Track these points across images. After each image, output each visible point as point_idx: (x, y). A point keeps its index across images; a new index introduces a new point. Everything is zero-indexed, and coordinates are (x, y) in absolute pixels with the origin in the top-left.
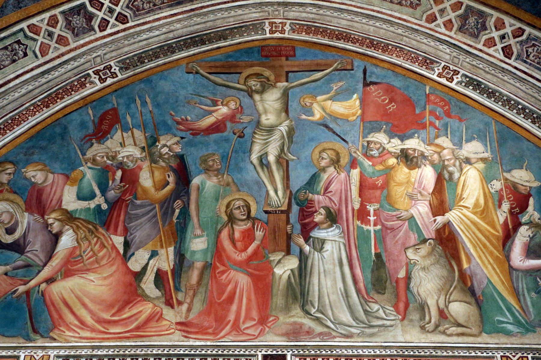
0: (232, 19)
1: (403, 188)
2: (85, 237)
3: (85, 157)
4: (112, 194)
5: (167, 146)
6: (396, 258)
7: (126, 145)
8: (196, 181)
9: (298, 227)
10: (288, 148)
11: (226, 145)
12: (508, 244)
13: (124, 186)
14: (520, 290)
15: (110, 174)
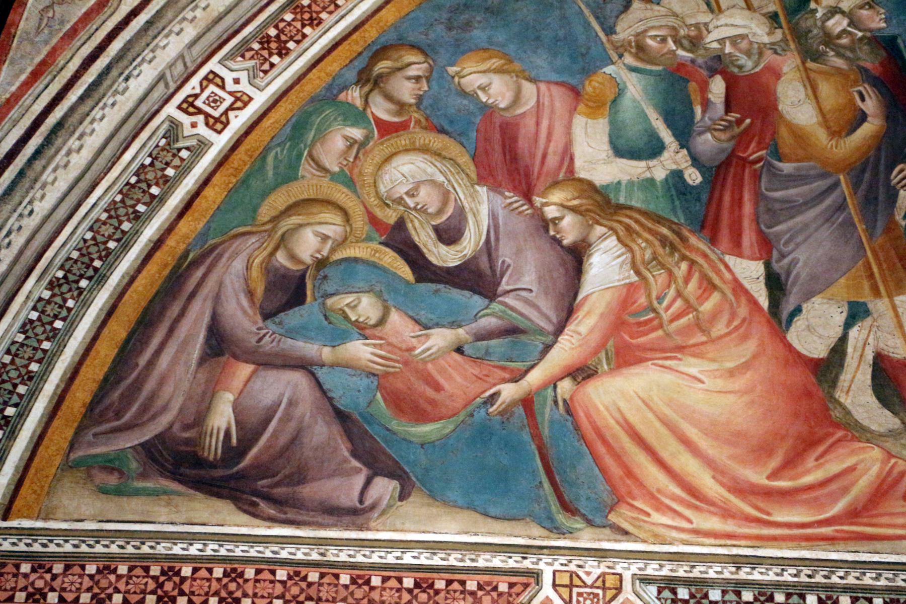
2: (655, 258)
3: (614, 37)
5: (843, 13)
7: (723, 7)
13: (739, 122)
15: (693, 86)
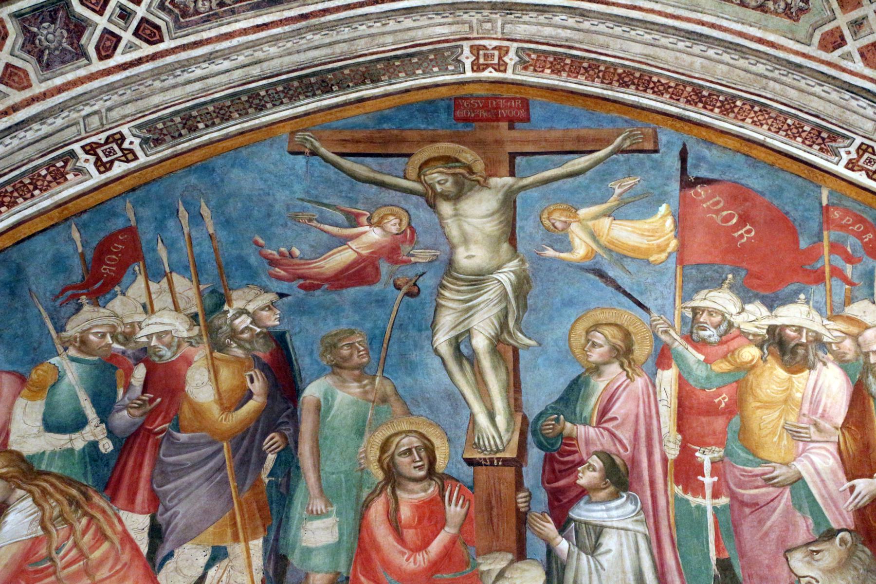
0: (389, 39)
1: (777, 414)
2: (61, 515)
3: (64, 334)
4: (123, 418)
5: (248, 313)
6: (766, 571)
7: (156, 308)
8: (312, 391)
9: (542, 497)
10: (518, 321)
11: (379, 312)
13: (151, 401)
15: (120, 372)
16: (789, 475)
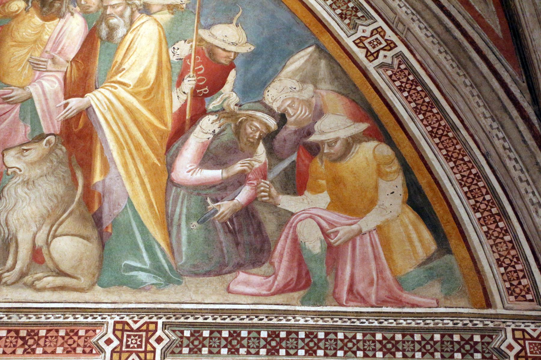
1: (26, 50)
12: (176, 145)
14: (176, 217)
16: (23, 95)
